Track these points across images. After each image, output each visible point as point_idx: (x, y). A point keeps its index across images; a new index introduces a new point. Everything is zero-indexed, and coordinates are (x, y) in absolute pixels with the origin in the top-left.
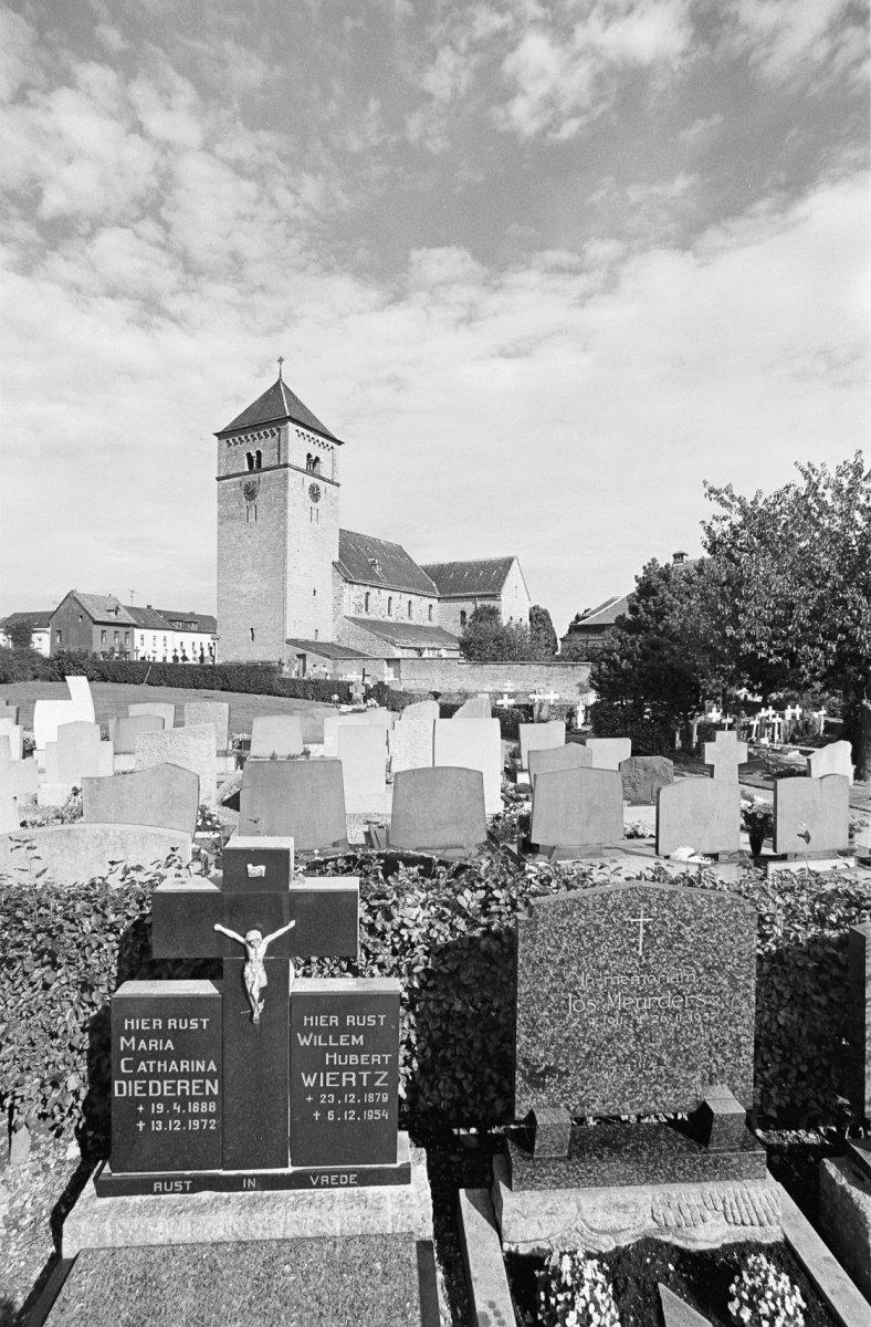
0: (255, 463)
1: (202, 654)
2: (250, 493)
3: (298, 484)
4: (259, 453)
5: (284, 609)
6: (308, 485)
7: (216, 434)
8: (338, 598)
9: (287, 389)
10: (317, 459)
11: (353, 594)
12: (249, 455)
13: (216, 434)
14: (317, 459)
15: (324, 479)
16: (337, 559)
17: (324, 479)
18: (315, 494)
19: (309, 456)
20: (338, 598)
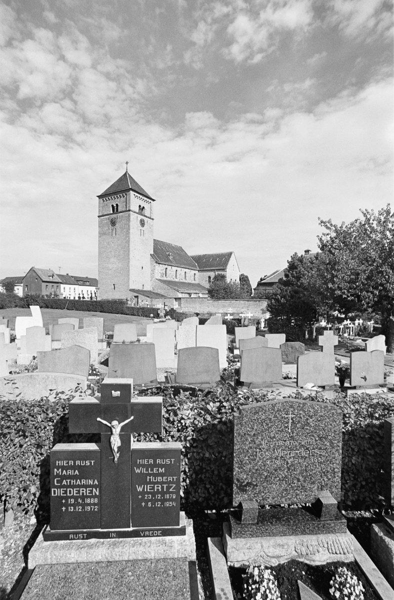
0: (115, 209)
1: (92, 296)
2: (113, 223)
3: (135, 219)
4: (117, 205)
5: (129, 275)
6: (139, 219)
7: (98, 196)
8: (153, 270)
9: (130, 176)
10: (144, 207)
11: (160, 269)
12: (113, 206)
13: (98, 196)
14: (144, 207)
15: (146, 217)
16: (152, 253)
17: (146, 217)
18: (142, 223)
19: (140, 206)
20: (153, 270)
